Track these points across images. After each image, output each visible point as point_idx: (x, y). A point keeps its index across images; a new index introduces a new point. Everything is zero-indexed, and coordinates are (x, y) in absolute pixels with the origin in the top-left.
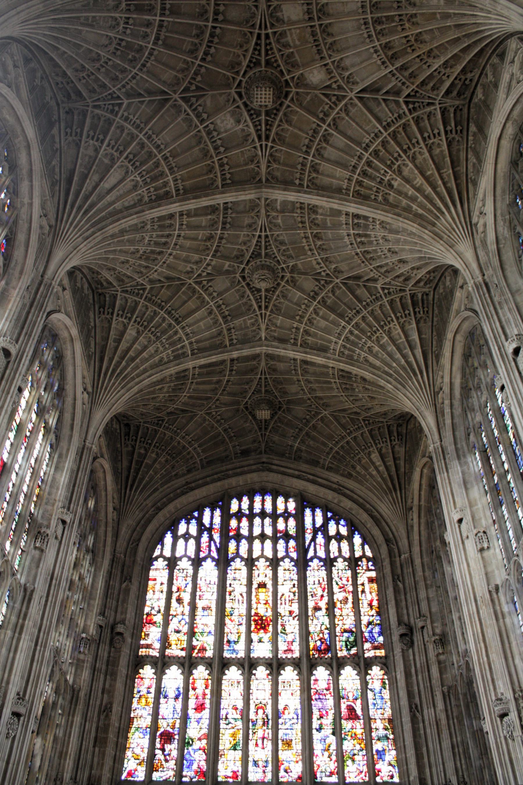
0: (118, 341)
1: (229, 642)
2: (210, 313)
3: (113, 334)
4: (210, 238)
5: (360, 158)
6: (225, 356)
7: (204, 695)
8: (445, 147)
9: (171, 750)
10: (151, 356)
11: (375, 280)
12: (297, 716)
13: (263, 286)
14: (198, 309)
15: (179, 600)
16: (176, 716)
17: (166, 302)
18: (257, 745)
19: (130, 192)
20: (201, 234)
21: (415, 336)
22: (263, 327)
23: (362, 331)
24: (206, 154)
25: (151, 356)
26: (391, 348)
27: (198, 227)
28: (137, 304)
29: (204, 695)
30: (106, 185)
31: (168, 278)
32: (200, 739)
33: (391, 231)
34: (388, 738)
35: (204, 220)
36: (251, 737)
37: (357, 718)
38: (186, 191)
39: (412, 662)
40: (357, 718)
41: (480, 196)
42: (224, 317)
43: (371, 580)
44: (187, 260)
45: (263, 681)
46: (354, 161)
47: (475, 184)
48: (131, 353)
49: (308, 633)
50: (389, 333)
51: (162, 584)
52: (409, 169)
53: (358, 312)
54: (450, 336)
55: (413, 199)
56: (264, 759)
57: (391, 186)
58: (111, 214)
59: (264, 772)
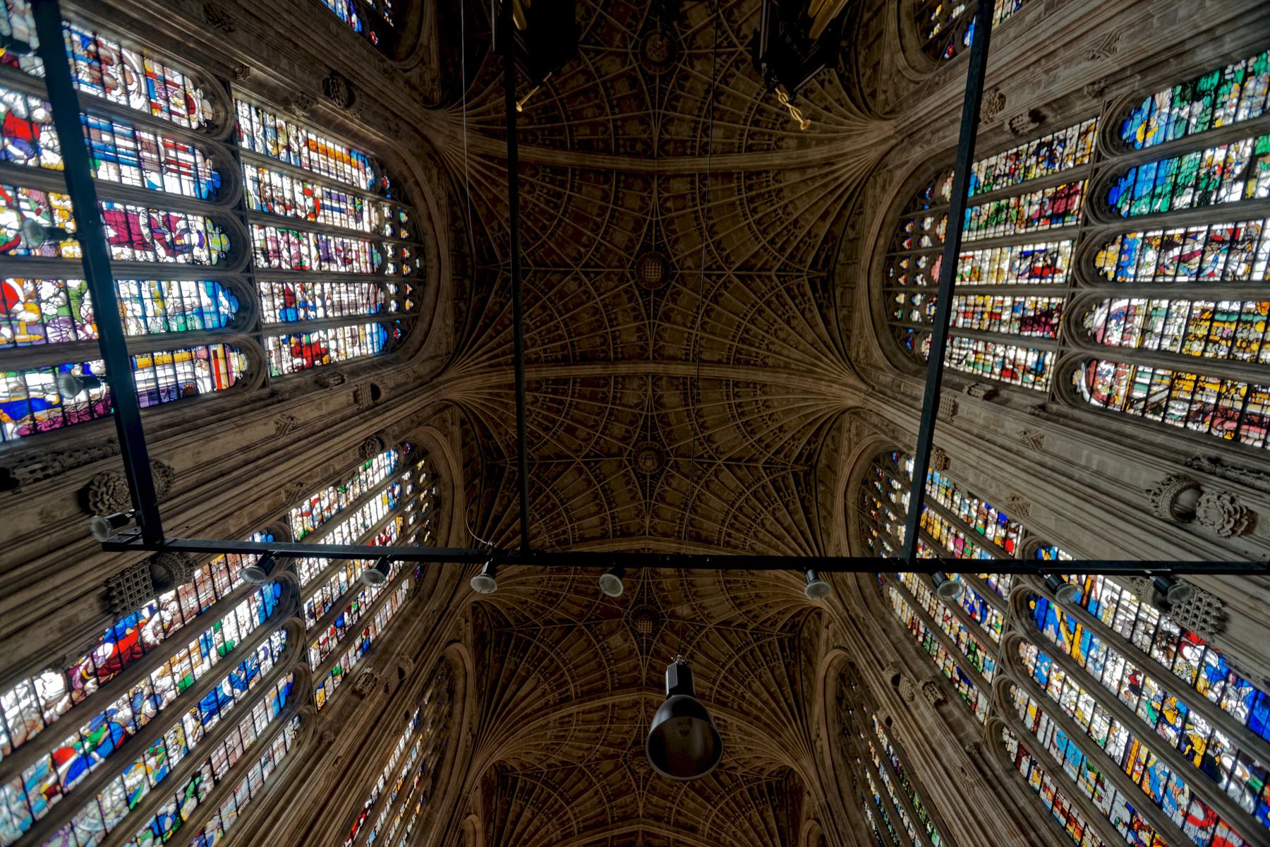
0: (515, 823)
2: (596, 793)
3: (511, 816)
4: (600, 730)
5: (719, 673)
6: (608, 835)
8: (783, 669)
10: (542, 838)
11: (734, 768)
13: (642, 771)
14: (586, 790)
17: (560, 784)
19: (539, 698)
20: (592, 727)
21: (773, 824)
22: (641, 805)
23: (727, 816)
24: (600, 665)
25: (542, 838)
26: (752, 834)
27: (590, 722)
28: (535, 786)
30: (521, 693)
31: (564, 763)
33: (747, 733)
35: (595, 716)
38: (583, 694)
41: (815, 719)
42: (608, 797)
44: (579, 748)
46: (714, 675)
47: (810, 705)
48: (525, 836)
50: (750, 819)
52: (756, 685)
53: (722, 797)
54: (803, 835)
55: (761, 710)
57: (744, 698)
58: (523, 718)
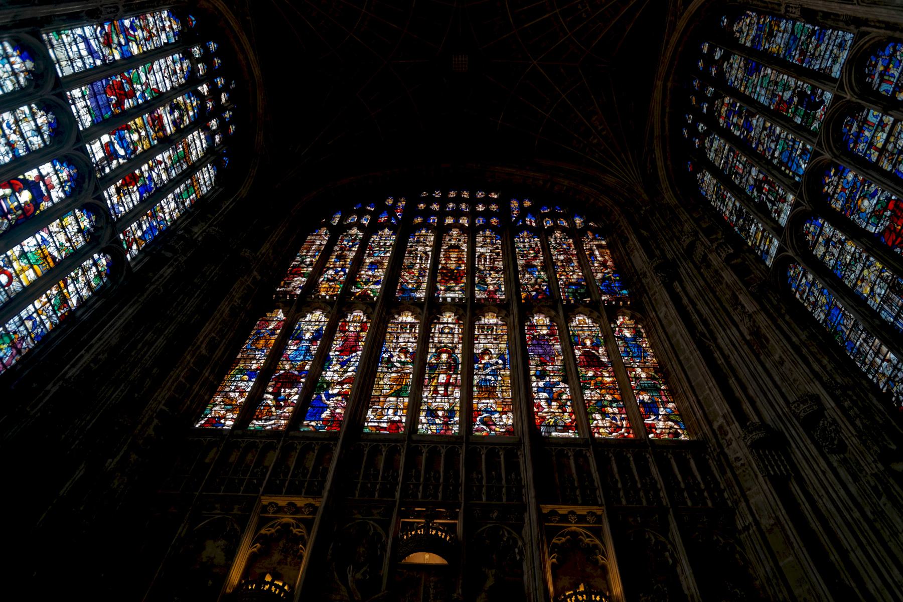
1: (403, 290)
7: (358, 338)
9: (290, 395)
12: (504, 360)
15: (341, 257)
16: (308, 358)
18: (436, 391)
29: (358, 338)
32: (341, 383)
34: (659, 390)
36: (426, 382)
37: (603, 365)
39: (682, 294)
40: (603, 365)
43: (599, 247)
45: (451, 326)
49: (518, 285)
51: (321, 245)
56: (447, 406)
59: (446, 424)
